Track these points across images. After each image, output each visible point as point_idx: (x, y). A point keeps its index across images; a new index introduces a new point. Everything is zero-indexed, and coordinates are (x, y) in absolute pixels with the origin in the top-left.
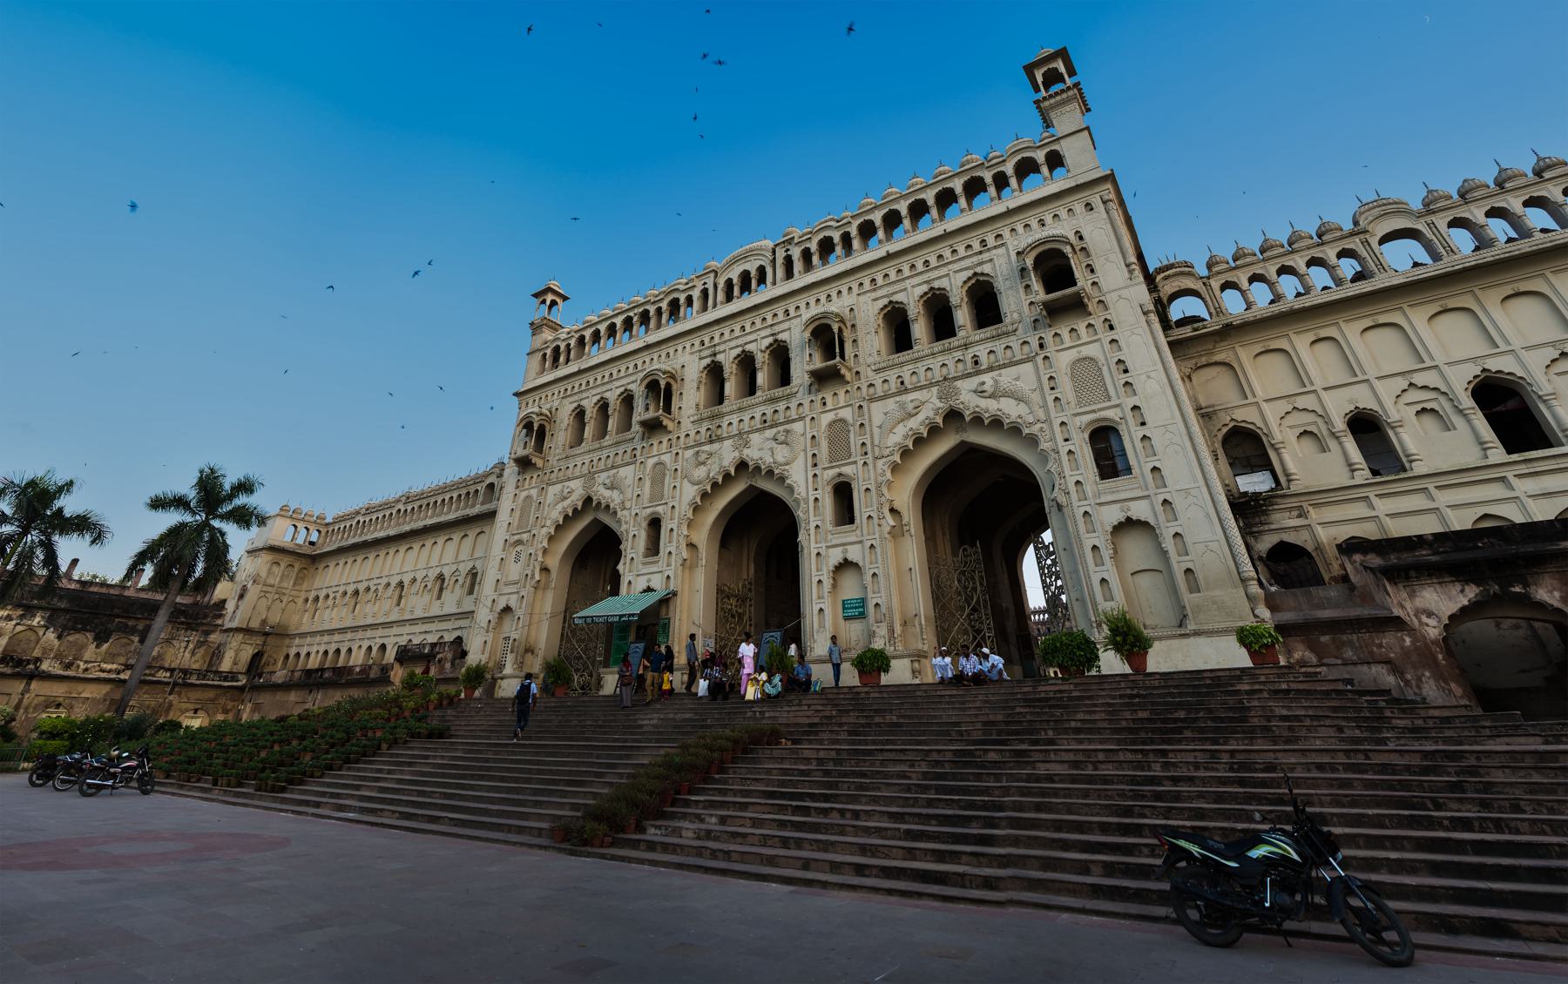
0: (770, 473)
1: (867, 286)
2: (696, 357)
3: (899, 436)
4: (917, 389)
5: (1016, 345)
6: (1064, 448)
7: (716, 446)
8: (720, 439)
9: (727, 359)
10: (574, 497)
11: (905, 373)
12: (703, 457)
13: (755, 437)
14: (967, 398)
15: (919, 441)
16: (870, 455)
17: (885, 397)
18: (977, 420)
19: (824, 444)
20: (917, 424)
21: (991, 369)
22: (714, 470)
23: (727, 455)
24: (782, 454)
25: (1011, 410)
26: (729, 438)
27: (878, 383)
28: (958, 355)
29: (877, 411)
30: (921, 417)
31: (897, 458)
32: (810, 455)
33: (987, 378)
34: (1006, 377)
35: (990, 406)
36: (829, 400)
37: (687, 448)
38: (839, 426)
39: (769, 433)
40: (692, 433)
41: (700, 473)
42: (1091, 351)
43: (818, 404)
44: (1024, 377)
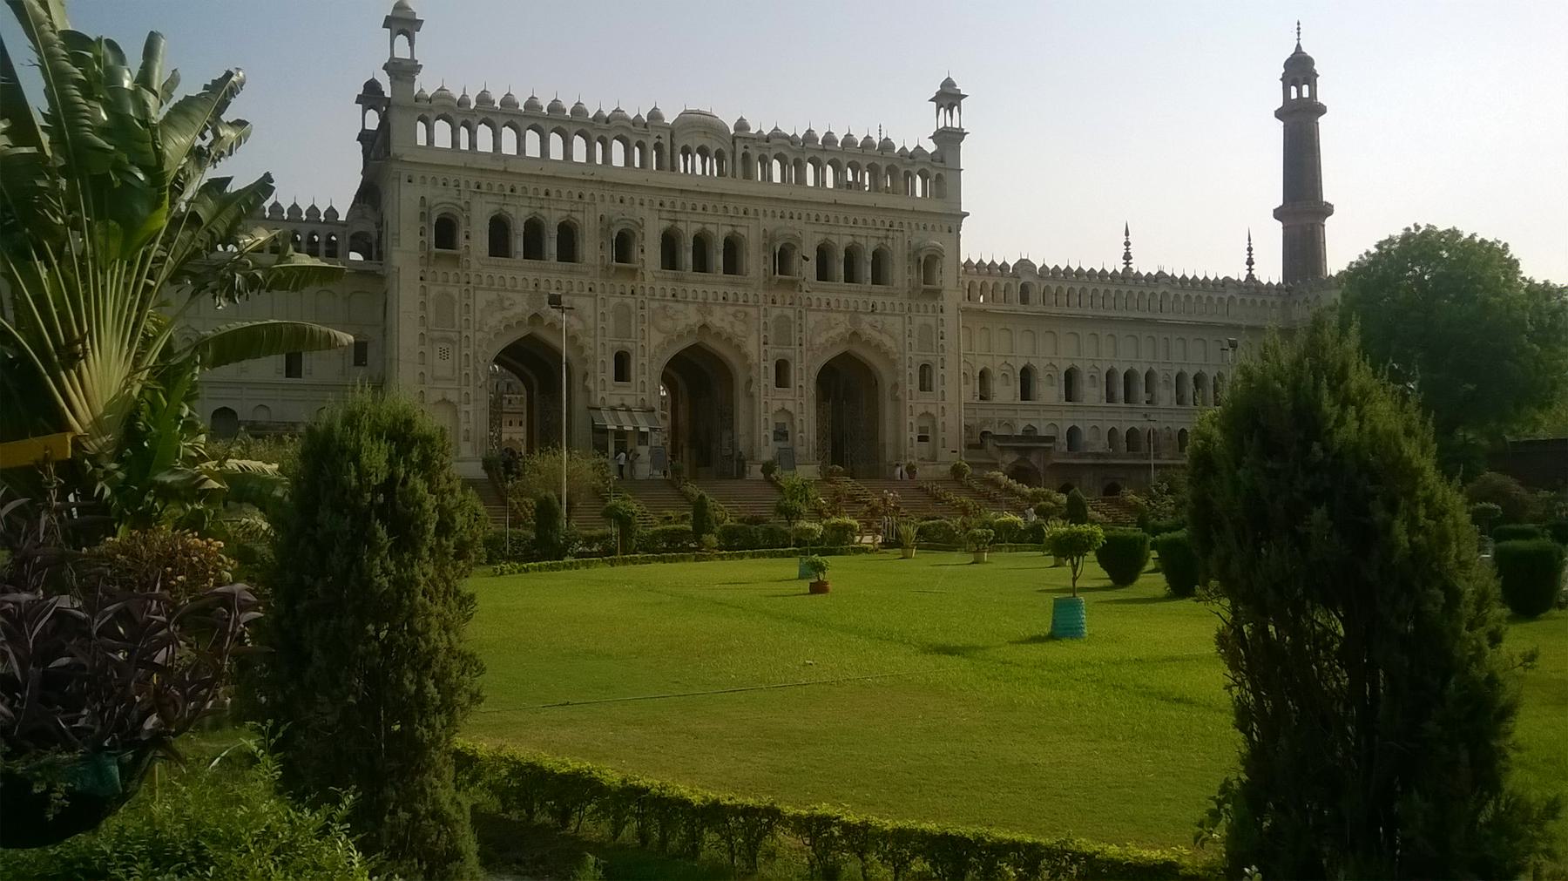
0: (729, 339)
5: (897, 303)
6: (908, 371)
7: (681, 306)
8: (686, 303)
10: (518, 309)
11: (833, 298)
12: (671, 312)
14: (866, 325)
18: (868, 342)
22: (681, 326)
24: (739, 328)
25: (888, 342)
28: (865, 298)
30: (838, 331)
36: (778, 300)
39: (731, 310)
41: (668, 324)
42: (932, 321)
44: (896, 324)
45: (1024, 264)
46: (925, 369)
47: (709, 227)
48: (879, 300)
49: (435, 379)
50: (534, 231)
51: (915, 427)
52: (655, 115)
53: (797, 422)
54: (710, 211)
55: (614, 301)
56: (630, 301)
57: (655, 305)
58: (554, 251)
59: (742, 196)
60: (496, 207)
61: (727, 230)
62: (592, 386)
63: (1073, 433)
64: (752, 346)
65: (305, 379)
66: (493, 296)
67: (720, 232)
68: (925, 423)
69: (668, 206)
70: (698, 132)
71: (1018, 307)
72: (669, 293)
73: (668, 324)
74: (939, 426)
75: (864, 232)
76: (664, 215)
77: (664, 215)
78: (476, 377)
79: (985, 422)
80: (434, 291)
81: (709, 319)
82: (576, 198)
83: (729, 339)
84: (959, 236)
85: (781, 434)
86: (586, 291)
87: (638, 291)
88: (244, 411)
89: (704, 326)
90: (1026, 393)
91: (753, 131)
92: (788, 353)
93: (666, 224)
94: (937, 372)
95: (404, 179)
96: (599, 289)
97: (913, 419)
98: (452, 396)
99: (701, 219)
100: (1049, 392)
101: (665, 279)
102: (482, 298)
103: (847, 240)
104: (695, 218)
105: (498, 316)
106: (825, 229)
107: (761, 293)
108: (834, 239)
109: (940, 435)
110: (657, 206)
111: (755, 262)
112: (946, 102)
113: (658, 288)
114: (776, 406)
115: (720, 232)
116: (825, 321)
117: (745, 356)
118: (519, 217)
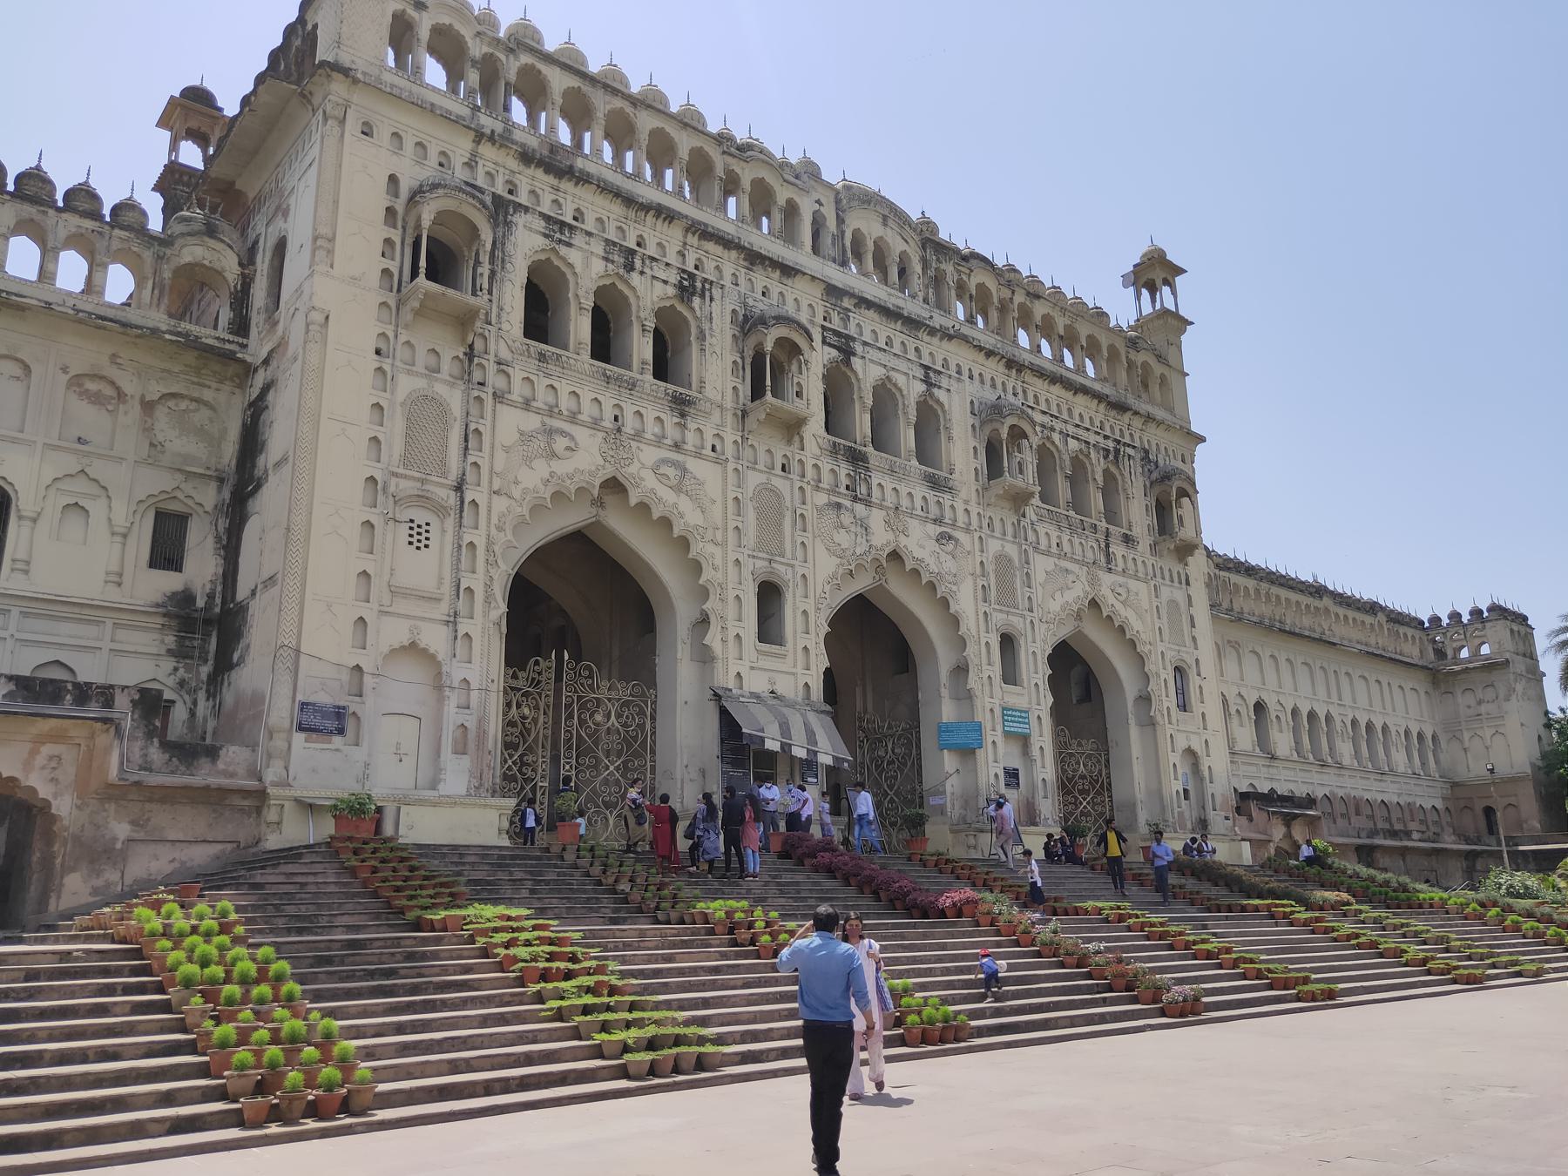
3: (1055, 606)
13: (914, 525)
26: (881, 507)
38: (1002, 560)
49: (395, 592)
54: (897, 349)
55: (754, 479)
56: (779, 483)
58: (648, 354)
62: (717, 647)
64: (965, 602)
66: (532, 422)
80: (406, 385)
81: (903, 541)
87: (795, 467)
95: (353, 126)
96: (730, 450)
102: (509, 423)
105: (542, 468)
117: (955, 621)
118: (587, 269)
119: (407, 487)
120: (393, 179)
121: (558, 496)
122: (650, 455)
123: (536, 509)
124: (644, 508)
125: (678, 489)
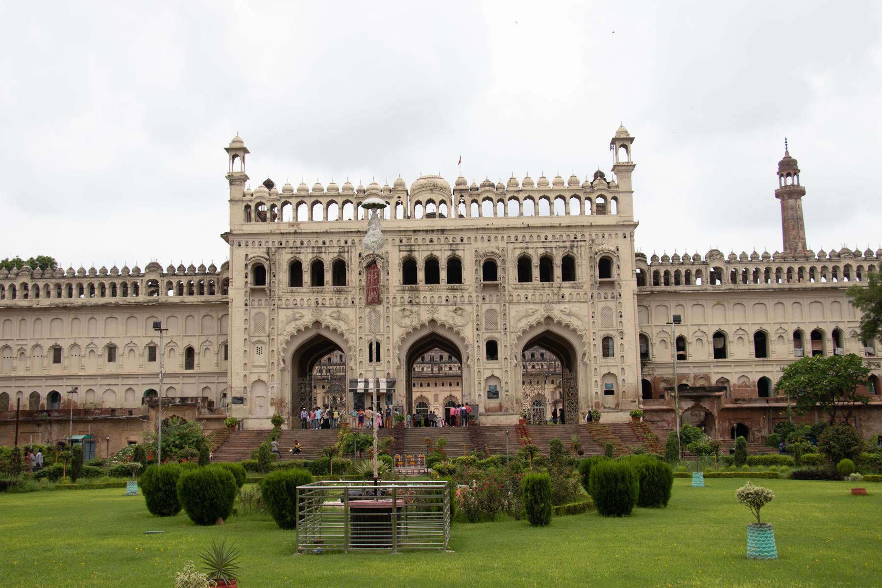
1: (513, 240)
2: (397, 249)
3: (523, 324)
4: (534, 303)
5: (582, 294)
6: (592, 342)
7: (415, 308)
8: (418, 304)
9: (421, 258)
13: (442, 309)
14: (557, 312)
15: (531, 327)
16: (508, 330)
17: (519, 303)
18: (559, 323)
19: (484, 320)
20: (532, 320)
21: (569, 302)
22: (416, 323)
23: (425, 316)
24: (459, 321)
25: (575, 323)
26: (425, 305)
27: (515, 295)
29: (514, 311)
30: (534, 317)
31: (520, 334)
32: (475, 324)
33: (566, 306)
34: (575, 308)
35: (566, 319)
36: (487, 298)
37: (395, 305)
40: (398, 297)
41: (407, 322)
43: (480, 299)
44: (583, 310)
45: (714, 254)
46: (607, 342)
47: (435, 253)
48: (566, 292)
49: (254, 367)
50: (317, 267)
51: (599, 383)
52: (400, 185)
53: (503, 384)
54: (435, 242)
57: (397, 309)
59: (458, 230)
60: (290, 256)
61: (448, 253)
63: (763, 383)
64: (468, 333)
65: (196, 370)
67: (443, 258)
68: (609, 381)
69: (405, 242)
70: (431, 191)
71: (731, 286)
72: (407, 300)
73: (407, 322)
74: (620, 382)
75: (554, 245)
76: (404, 248)
77: (404, 248)
78: (279, 364)
79: (683, 376)
80: (254, 311)
81: (436, 316)
82: (342, 244)
83: (451, 329)
84: (632, 241)
85: (493, 394)
86: (350, 304)
88: (162, 393)
89: (433, 321)
90: (720, 353)
91: (469, 185)
92: (496, 336)
93: (405, 254)
94: (617, 342)
97: (599, 379)
98: (264, 377)
99: (430, 248)
100: (741, 349)
101: (403, 291)
103: (541, 251)
104: (425, 248)
105: (293, 324)
106: (524, 245)
107: (474, 295)
108: (530, 252)
109: (621, 389)
110: (397, 242)
111: (471, 273)
112: (618, 144)
113: (398, 297)
114: (488, 373)
115: (443, 258)
116: (526, 308)
117: (463, 339)
119: (255, 339)
120: (247, 255)
121: (299, 331)
122: (328, 311)
123: (292, 336)
124: (327, 327)
125: (338, 319)
